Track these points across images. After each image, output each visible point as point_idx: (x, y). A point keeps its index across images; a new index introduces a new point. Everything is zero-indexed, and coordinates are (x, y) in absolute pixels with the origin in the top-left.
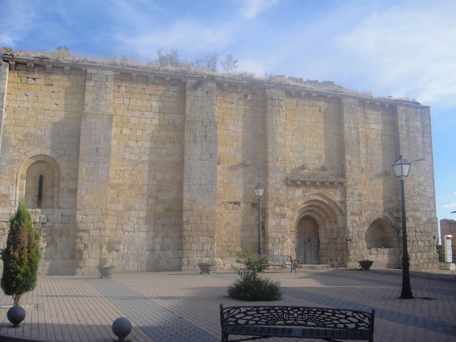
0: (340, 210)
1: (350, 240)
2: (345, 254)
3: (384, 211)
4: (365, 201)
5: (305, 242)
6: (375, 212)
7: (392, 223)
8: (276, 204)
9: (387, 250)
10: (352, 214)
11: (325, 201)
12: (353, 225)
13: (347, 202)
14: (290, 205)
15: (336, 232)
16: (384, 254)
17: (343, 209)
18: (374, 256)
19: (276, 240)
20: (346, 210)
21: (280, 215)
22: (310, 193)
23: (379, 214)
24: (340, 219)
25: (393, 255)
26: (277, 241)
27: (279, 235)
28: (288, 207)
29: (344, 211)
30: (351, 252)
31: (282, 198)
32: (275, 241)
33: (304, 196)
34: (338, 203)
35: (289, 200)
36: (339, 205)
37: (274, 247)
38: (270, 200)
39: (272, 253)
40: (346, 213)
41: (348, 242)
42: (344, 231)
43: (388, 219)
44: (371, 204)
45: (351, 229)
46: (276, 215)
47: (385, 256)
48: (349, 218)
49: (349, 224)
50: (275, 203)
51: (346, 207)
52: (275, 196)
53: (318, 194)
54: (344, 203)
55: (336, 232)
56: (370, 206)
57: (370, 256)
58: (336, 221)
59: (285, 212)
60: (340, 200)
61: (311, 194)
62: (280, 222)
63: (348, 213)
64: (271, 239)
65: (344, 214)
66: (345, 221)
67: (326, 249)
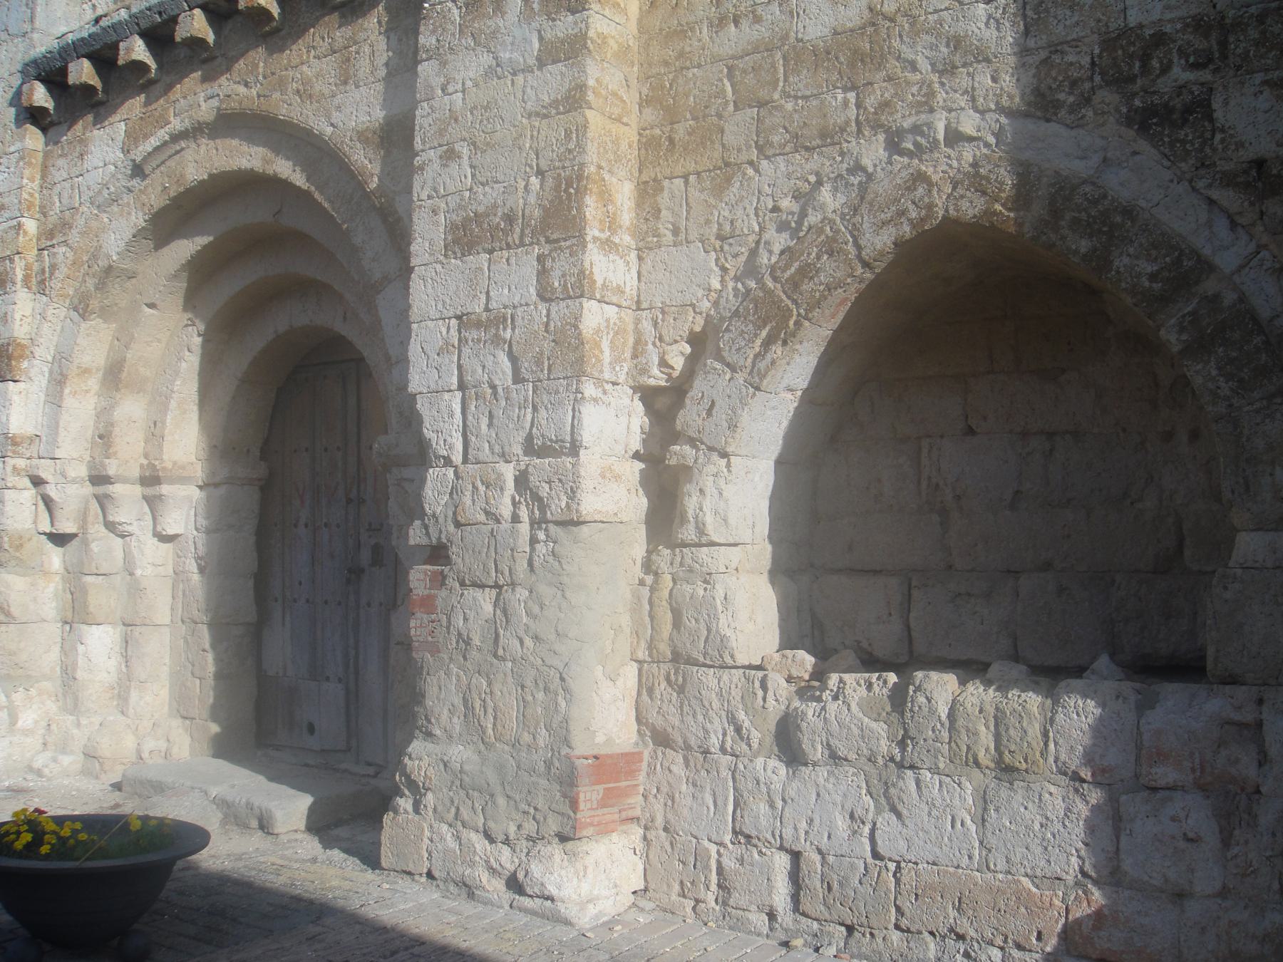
3: (1041, 104)
4: (733, 39)
6: (872, 152)
7: (1184, 271)
9: (1078, 717)
11: (284, 168)
16: (1006, 771)
18: (849, 788)
22: (162, 134)
23: (940, 167)
25: (1197, 815)
43: (1111, 222)
44: (820, 56)
47: (1015, 799)
53: (230, 123)
54: (396, 137)
56: (802, 82)
57: (773, 770)
61: (176, 138)
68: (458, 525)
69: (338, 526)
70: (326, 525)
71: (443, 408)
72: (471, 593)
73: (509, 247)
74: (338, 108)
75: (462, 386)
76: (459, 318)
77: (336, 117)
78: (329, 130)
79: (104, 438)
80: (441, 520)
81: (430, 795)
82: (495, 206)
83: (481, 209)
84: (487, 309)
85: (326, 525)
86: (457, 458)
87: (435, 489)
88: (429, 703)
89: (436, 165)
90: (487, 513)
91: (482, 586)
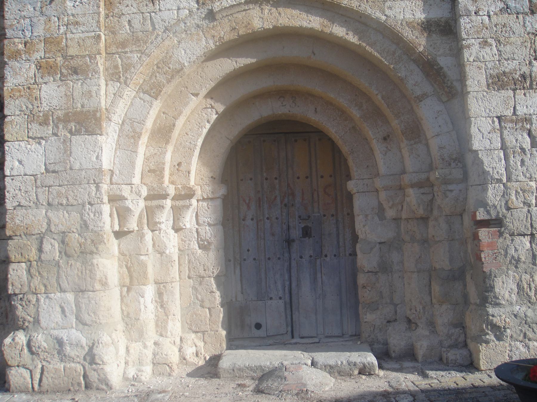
0: (430, 69)
1: (497, 223)
2: (474, 297)
5: (289, 242)
8: (46, 68)
10: (499, 81)
11: (339, 31)
12: (511, 140)
13: (464, 22)
14: (127, 68)
15: (419, 185)
17: (445, 62)
19: (47, 247)
20: (460, 66)
21: (66, 119)
24: (429, 112)
26: (52, 248)
27: (62, 219)
28: (114, 75)
29: (452, 74)
30: (505, 287)
31: (77, 34)
32: (40, 250)
33: (211, 15)
34: (409, 35)
35: (123, 44)
36: (420, 42)
37: (36, 281)
38: (16, 55)
39: (32, 309)
40: (462, 78)
41: (483, 233)
42: (457, 174)
45: (494, 164)
46: (44, 123)
48: (483, 107)
49: (483, 137)
50: (39, 67)
51: (457, 52)
52: (40, 31)
55: (419, 185)
58: (415, 132)
59: (90, 105)
60: (421, 16)
62: (67, 152)
63: (476, 80)
64: (25, 240)
65: (448, 85)
66: (459, 123)
67: (384, 268)
68: (508, 209)
69: (277, 218)
70: (268, 219)
71: (495, 156)
72: (517, 239)
73: (524, 88)
74: (390, 8)
75: (504, 147)
76: (498, 117)
77: (387, 12)
78: (384, 18)
79: (155, 171)
80: (498, 207)
81: (508, 331)
82: (515, 70)
83: (507, 70)
84: (514, 113)
85: (268, 219)
86: (505, 180)
87: (493, 194)
88: (497, 290)
89: (477, 46)
90: (524, 203)
91: (524, 235)
